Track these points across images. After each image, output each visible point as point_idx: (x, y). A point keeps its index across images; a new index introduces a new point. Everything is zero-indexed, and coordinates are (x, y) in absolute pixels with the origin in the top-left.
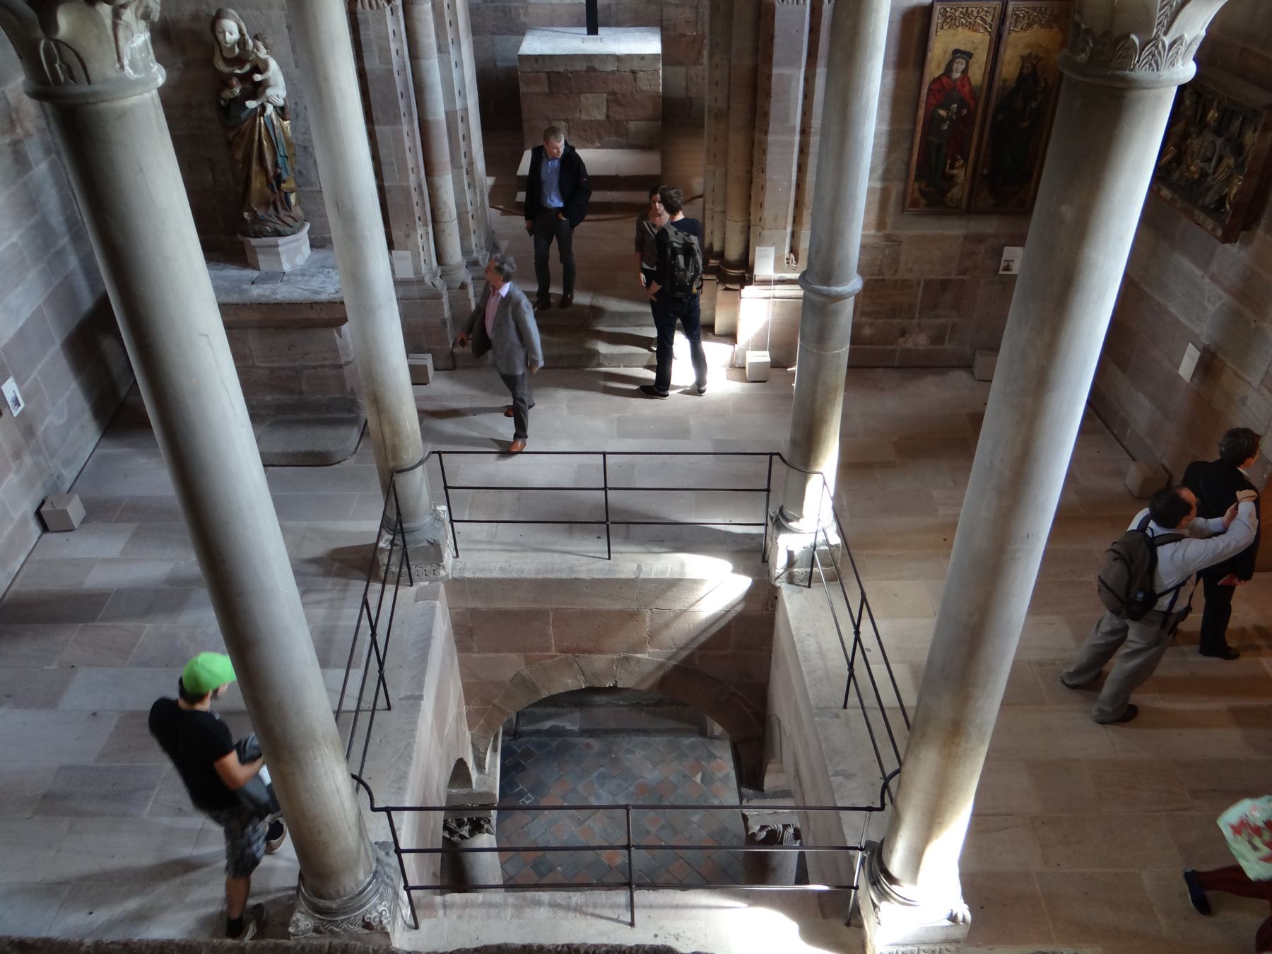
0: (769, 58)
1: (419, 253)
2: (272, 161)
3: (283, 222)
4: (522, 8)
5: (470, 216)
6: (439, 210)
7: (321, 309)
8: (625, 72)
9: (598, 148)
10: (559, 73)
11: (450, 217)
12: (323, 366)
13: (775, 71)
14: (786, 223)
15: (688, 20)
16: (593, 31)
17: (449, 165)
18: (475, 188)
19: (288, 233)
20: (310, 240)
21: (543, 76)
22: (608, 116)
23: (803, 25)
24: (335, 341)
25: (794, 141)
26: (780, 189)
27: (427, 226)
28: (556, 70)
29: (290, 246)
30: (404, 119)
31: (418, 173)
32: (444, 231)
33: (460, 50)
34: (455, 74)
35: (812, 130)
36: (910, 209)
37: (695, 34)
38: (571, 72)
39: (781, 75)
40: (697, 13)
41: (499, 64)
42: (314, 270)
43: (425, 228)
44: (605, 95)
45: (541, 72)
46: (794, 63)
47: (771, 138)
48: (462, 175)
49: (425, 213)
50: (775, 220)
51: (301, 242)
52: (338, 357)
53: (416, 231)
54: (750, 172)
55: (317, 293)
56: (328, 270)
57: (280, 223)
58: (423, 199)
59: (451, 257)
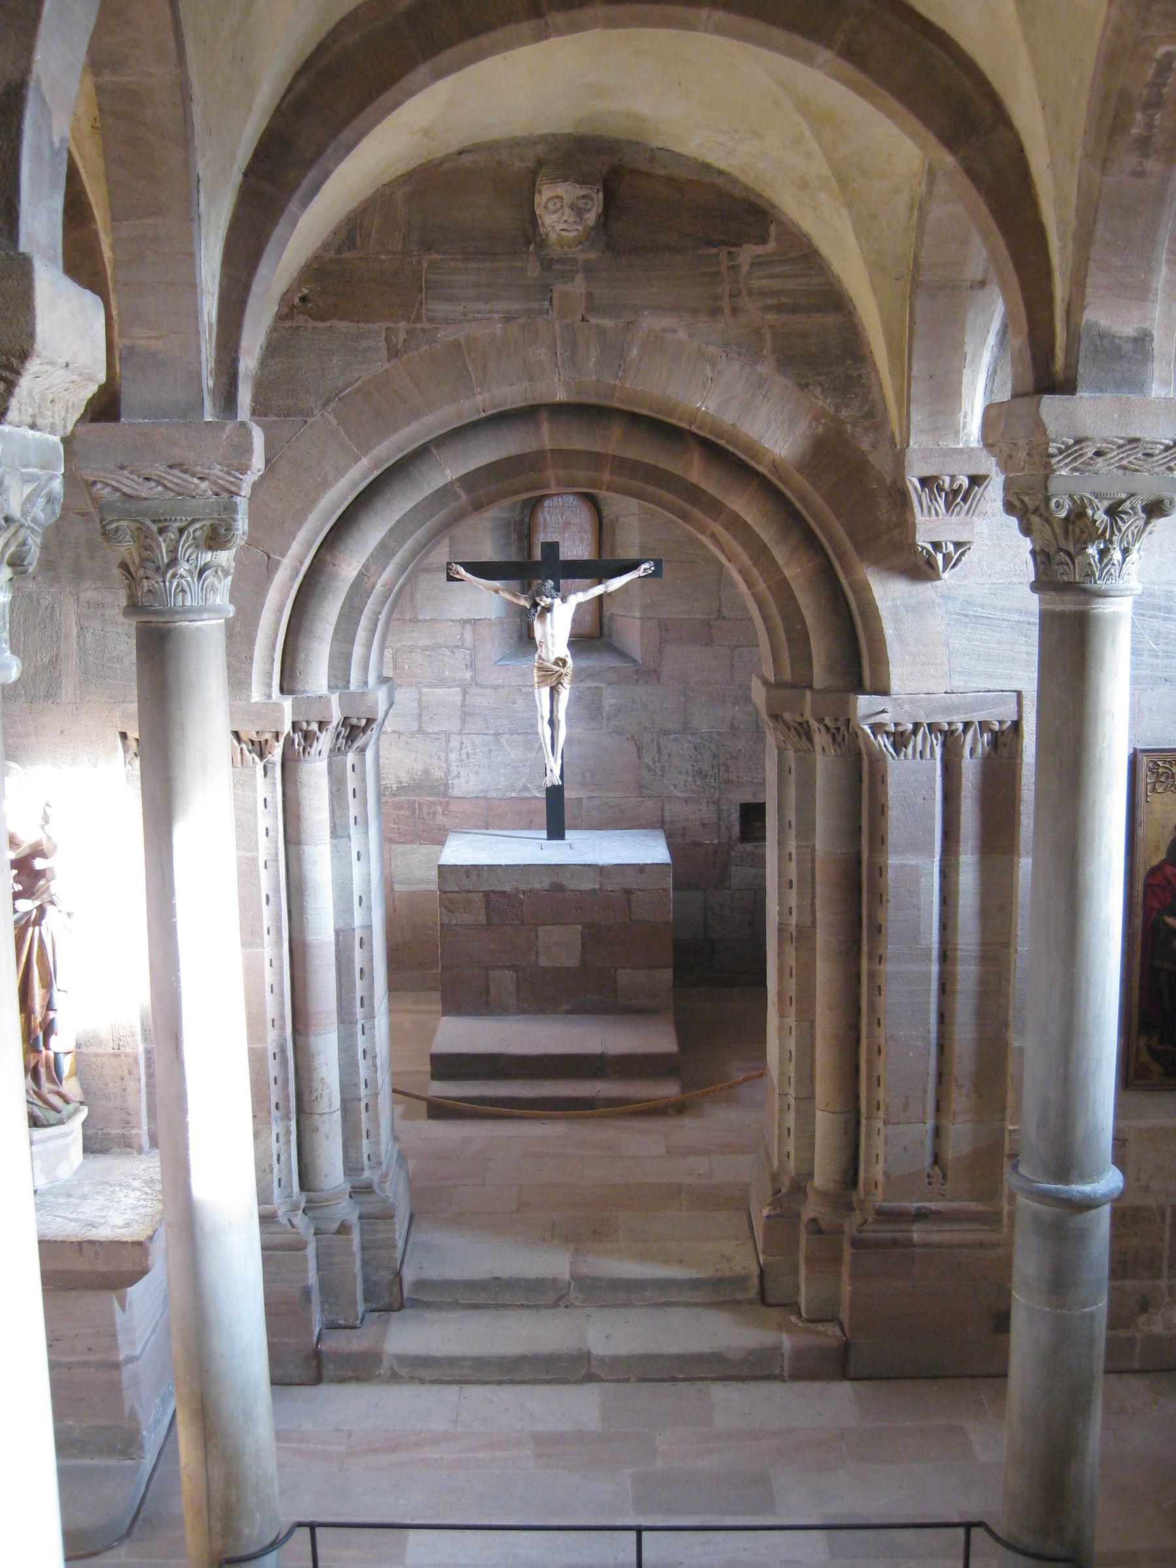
0: (879, 841)
1: (271, 1165)
2: (44, 999)
3: (46, 1102)
4: (440, 803)
6: (311, 1092)
7: (96, 1253)
8: (612, 891)
9: (567, 1012)
10: (504, 892)
11: (330, 1105)
12: (86, 1364)
13: (893, 860)
14: (924, 1112)
15: (704, 821)
16: (556, 831)
19: (52, 1122)
20: (84, 1139)
21: (477, 897)
22: (582, 960)
23: (933, 788)
24: (112, 1317)
25: (930, 973)
26: (911, 1054)
27: (289, 1119)
28: (497, 889)
29: (52, 1144)
30: (267, 938)
31: (283, 1028)
32: (317, 1129)
33: (366, 833)
34: (357, 870)
35: (959, 953)
36: (1137, 1082)
37: (716, 842)
38: (524, 893)
39: (903, 866)
40: (719, 811)
41: (397, 887)
42: (86, 1189)
43: (285, 1123)
44: (580, 927)
45: (475, 892)
46: (923, 848)
47: (889, 967)
48: (353, 1035)
49: (287, 1097)
50: (905, 1108)
51: (71, 1138)
52: (114, 1347)
53: (270, 1128)
54: (855, 1028)
55: (92, 1225)
56: (111, 1189)
57: (40, 1103)
58: (286, 1072)
59: (326, 1176)
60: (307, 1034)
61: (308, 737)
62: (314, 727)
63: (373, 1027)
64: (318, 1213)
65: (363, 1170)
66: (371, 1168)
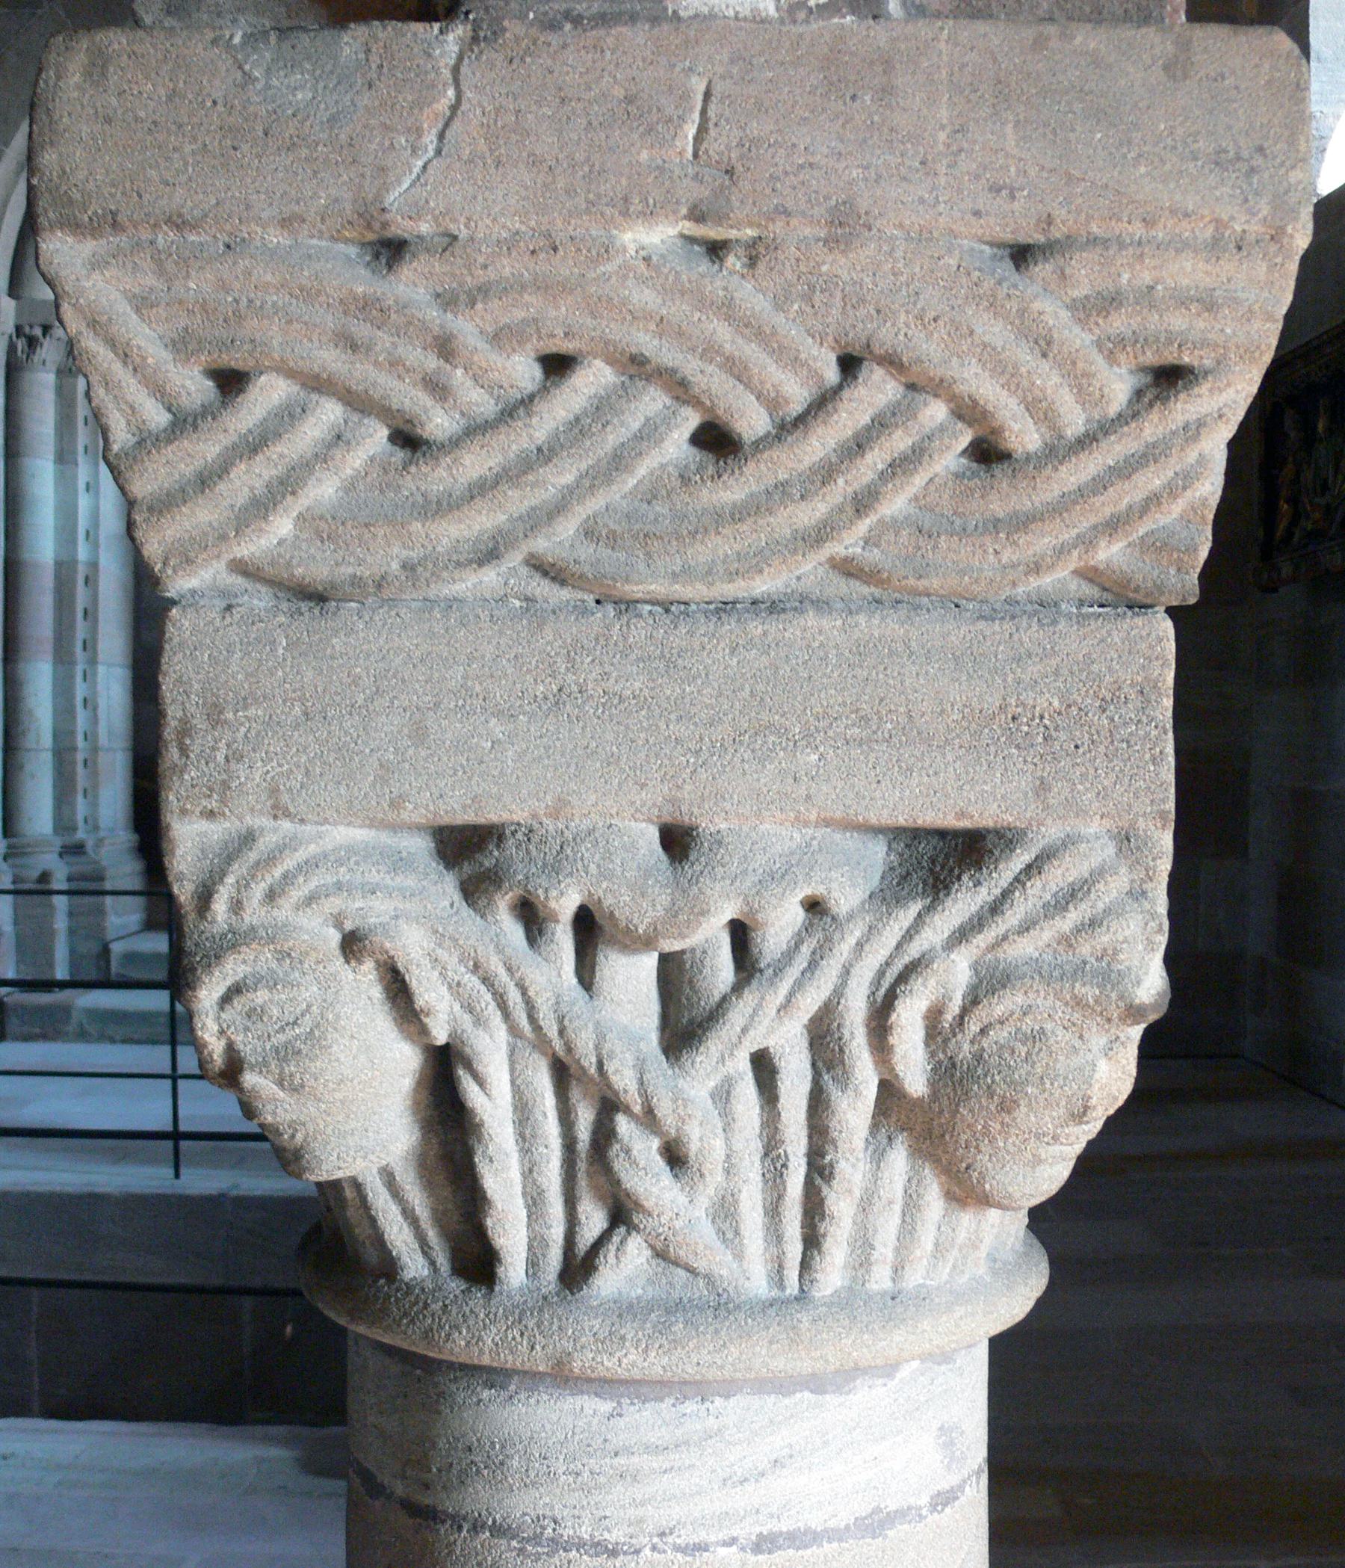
5: (80, 757)
11: (38, 742)
17: (48, 647)
18: (95, 708)
32: (22, 767)
34: (84, 502)
60: (15, 661)
61: (32, 343)
62: (38, 332)
63: (95, 674)
64: (18, 861)
65: (75, 829)
66: (88, 832)
